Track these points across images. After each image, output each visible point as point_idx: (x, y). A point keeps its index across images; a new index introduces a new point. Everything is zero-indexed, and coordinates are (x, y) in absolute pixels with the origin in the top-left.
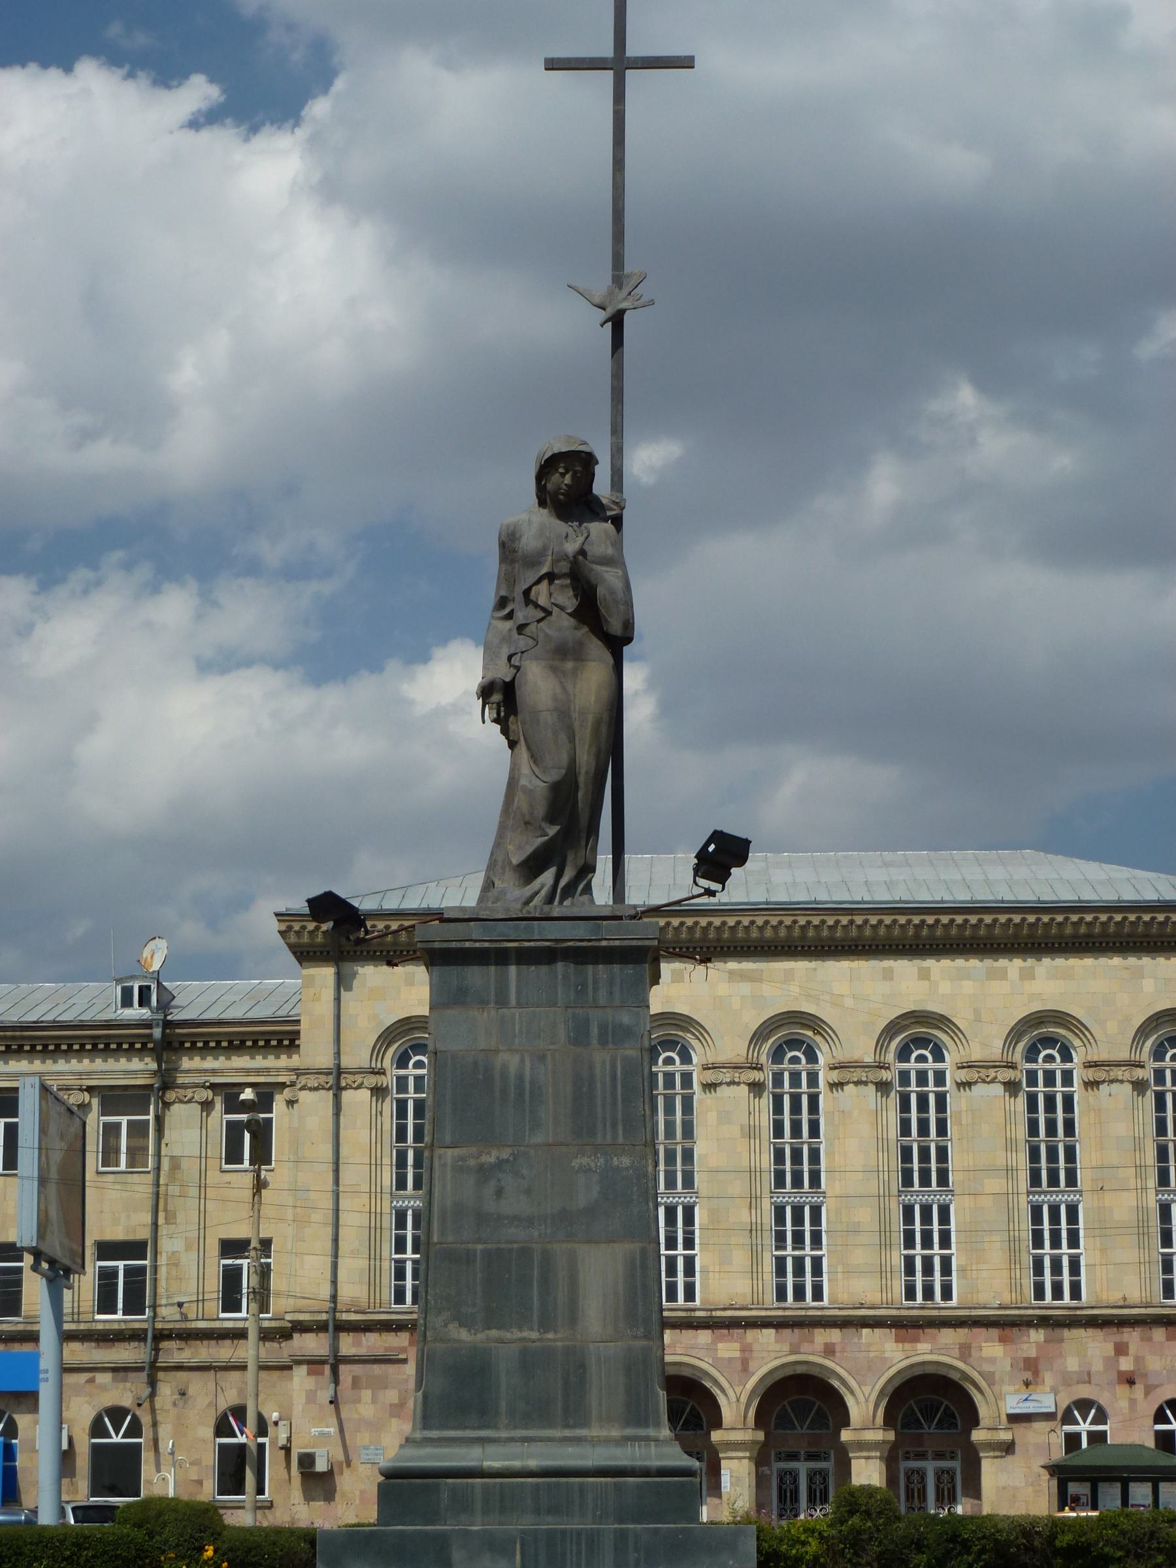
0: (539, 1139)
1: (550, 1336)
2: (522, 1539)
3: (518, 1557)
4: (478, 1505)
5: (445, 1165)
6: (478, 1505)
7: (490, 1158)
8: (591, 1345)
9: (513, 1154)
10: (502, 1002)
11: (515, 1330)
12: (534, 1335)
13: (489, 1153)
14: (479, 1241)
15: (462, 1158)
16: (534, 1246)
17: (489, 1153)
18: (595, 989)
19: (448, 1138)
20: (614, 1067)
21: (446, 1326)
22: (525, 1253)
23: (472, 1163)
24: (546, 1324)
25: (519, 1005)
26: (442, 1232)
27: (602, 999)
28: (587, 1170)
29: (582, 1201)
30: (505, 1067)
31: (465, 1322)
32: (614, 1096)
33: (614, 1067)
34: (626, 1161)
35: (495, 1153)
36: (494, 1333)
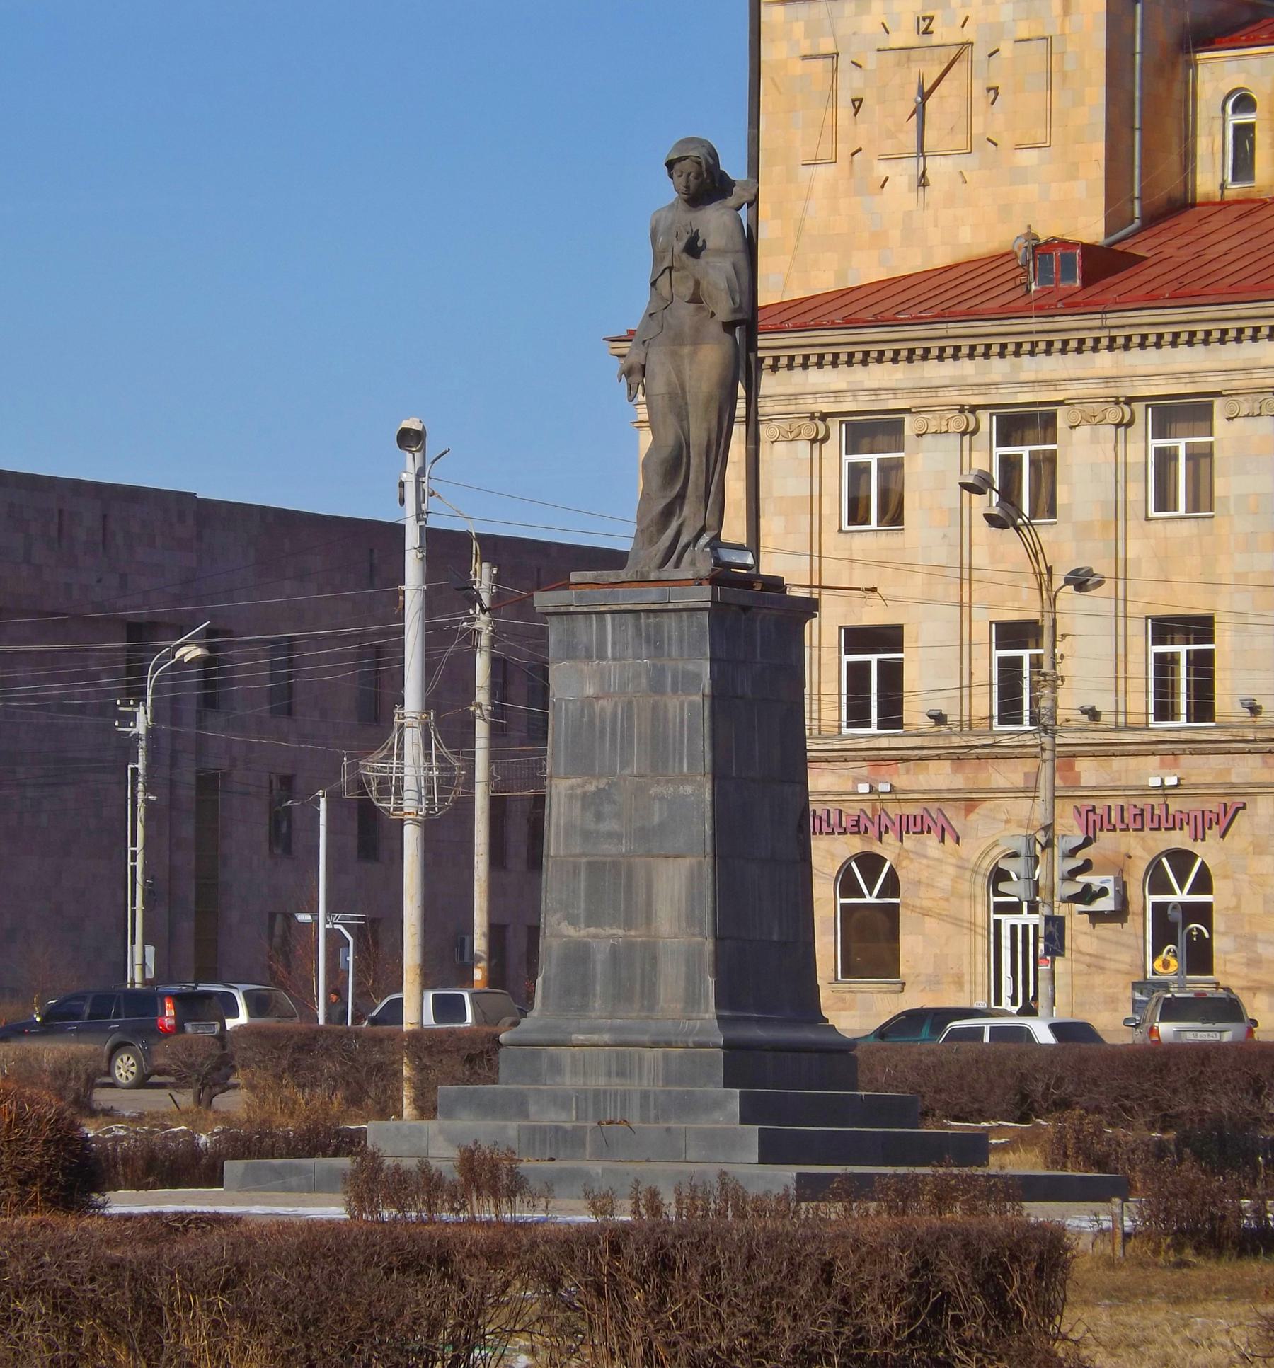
0: (627, 772)
1: (633, 933)
2: (577, 1098)
3: (574, 1112)
4: (568, 1069)
5: (559, 793)
6: (568, 1069)
7: (591, 788)
8: (661, 941)
9: (608, 784)
10: (602, 656)
11: (607, 928)
12: (621, 932)
13: (591, 783)
14: (584, 855)
15: (572, 788)
16: (621, 859)
17: (591, 783)
18: (669, 645)
19: (562, 770)
20: (682, 709)
21: (559, 924)
22: (615, 864)
23: (579, 791)
24: (628, 924)
25: (614, 659)
26: (557, 849)
27: (675, 652)
28: (662, 798)
29: (656, 820)
30: (603, 709)
31: (573, 921)
32: (682, 735)
33: (682, 709)
34: (688, 789)
35: (595, 783)
36: (592, 930)
